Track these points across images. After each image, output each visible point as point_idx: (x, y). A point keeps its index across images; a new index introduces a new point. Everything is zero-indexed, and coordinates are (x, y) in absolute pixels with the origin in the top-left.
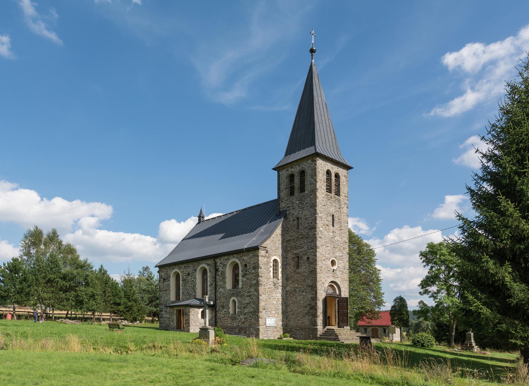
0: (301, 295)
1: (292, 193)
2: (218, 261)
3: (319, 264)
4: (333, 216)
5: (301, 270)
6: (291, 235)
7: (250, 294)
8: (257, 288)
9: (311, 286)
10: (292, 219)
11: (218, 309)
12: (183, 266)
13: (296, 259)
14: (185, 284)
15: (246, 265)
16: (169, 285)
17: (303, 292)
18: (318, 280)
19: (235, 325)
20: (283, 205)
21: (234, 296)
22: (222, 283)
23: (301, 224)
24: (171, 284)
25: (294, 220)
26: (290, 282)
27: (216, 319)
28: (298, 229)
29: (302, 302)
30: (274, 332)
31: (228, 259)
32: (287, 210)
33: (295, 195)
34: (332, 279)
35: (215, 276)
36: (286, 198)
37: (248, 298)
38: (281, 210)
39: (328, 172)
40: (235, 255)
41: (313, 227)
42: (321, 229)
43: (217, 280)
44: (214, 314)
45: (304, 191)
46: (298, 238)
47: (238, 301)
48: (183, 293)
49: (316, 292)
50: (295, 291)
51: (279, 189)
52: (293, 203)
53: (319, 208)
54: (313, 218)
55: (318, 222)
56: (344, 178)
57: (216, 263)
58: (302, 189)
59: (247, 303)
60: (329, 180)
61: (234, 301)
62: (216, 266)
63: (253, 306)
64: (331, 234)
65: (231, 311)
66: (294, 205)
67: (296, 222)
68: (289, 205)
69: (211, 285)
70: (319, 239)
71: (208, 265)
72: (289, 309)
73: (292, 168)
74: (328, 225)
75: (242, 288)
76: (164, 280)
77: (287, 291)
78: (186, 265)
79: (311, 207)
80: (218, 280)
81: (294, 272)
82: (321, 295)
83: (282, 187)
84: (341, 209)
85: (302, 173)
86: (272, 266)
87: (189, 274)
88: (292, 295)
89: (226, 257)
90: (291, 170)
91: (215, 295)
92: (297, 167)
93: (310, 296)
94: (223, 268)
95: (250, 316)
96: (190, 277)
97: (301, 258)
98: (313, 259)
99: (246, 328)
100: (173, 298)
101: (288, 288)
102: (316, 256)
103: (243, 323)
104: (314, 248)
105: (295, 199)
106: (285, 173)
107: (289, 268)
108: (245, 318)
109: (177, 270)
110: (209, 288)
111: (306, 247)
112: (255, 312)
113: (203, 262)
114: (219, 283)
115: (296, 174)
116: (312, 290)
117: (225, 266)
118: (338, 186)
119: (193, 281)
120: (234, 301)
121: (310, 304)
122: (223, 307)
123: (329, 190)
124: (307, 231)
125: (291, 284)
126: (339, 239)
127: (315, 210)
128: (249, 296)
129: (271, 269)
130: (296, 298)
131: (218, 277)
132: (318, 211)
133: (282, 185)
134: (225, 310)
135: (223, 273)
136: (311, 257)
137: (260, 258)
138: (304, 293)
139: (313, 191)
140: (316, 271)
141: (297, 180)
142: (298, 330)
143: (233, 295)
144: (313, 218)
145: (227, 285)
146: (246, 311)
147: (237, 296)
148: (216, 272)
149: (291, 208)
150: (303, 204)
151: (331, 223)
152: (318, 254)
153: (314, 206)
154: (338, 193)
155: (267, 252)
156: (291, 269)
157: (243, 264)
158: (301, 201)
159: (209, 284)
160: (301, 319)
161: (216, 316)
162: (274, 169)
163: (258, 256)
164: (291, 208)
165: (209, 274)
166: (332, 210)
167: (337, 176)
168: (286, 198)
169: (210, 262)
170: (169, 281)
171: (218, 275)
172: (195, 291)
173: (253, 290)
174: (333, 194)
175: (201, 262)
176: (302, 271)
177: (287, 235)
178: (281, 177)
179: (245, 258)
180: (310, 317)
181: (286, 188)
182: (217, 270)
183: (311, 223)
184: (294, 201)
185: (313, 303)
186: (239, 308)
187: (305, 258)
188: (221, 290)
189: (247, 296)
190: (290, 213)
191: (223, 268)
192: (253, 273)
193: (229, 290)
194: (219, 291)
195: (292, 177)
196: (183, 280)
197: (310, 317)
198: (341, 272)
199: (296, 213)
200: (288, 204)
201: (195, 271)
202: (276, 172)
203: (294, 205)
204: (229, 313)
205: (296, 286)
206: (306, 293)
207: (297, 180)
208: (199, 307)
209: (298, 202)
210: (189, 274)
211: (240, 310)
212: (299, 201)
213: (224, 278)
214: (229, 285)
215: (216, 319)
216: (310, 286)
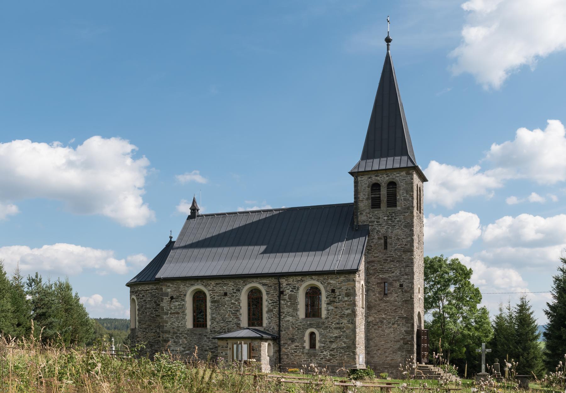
0: (390, 327)
2: (284, 282)
5: (391, 298)
6: (376, 255)
7: (341, 325)
8: (353, 320)
9: (405, 318)
10: (376, 237)
11: (282, 342)
12: (213, 283)
13: (382, 285)
15: (333, 291)
16: (183, 307)
17: (393, 324)
20: (362, 218)
21: (311, 327)
22: (291, 310)
23: (391, 244)
24: (187, 305)
25: (379, 239)
26: (373, 311)
32: (369, 225)
33: (382, 208)
36: (367, 211)
38: (360, 224)
40: (313, 277)
43: (282, 306)
44: (277, 349)
45: (396, 206)
46: (387, 260)
47: (320, 334)
48: (213, 319)
50: (382, 322)
51: (356, 197)
52: (379, 218)
54: (409, 239)
57: (280, 284)
59: (336, 337)
61: (312, 335)
62: (280, 288)
63: (345, 340)
65: (307, 345)
66: (381, 220)
67: (382, 241)
68: (373, 219)
69: (269, 311)
71: (264, 285)
73: (376, 176)
75: (327, 318)
76: (172, 298)
77: (369, 322)
78: (218, 281)
79: (405, 226)
82: (415, 330)
83: (361, 196)
85: (392, 185)
89: (299, 278)
90: (374, 179)
91: (279, 326)
92: (385, 176)
93: (403, 329)
96: (227, 299)
97: (391, 284)
98: (408, 286)
99: (335, 366)
100: (189, 324)
101: (371, 319)
102: (413, 283)
103: (329, 361)
106: (365, 181)
107: (372, 294)
108: (330, 355)
109: (199, 286)
110: (265, 315)
111: (397, 272)
112: (348, 347)
113: (255, 280)
114: (285, 310)
116: (407, 323)
119: (232, 303)
120: (312, 335)
121: (403, 339)
122: (293, 341)
124: (399, 254)
125: (376, 313)
128: (340, 328)
130: (384, 331)
131: (282, 302)
133: (361, 194)
134: (297, 344)
136: (405, 285)
137: (357, 284)
138: (396, 326)
139: (408, 208)
141: (384, 192)
142: (387, 368)
143: (311, 326)
145: (299, 313)
146: (334, 346)
147: (318, 327)
148: (279, 297)
149: (375, 223)
156: (376, 296)
157: (329, 288)
158: (391, 217)
159: (265, 309)
160: (391, 355)
161: (279, 351)
163: (354, 281)
164: (375, 223)
165: (265, 297)
168: (367, 211)
170: (183, 300)
171: (284, 300)
173: (346, 321)
175: (249, 280)
176: (392, 299)
177: (370, 256)
178: (359, 184)
179: (332, 282)
180: (404, 353)
181: (367, 199)
182: (281, 293)
183: (406, 245)
184: (381, 215)
185: (408, 338)
186: (320, 342)
187: (397, 284)
189: (336, 328)
190: (375, 229)
191: (291, 291)
192: (346, 301)
193: (303, 319)
195: (376, 187)
196: (212, 302)
197: (404, 353)
199: (383, 231)
200: (370, 218)
202: (352, 179)
203: (381, 220)
204: (304, 348)
205: (384, 316)
206: (399, 325)
207: (384, 192)
208: (266, 340)
209: (386, 218)
210: (226, 294)
211: (323, 345)
212: (388, 216)
214: (302, 313)
215: (280, 355)
216: (403, 318)
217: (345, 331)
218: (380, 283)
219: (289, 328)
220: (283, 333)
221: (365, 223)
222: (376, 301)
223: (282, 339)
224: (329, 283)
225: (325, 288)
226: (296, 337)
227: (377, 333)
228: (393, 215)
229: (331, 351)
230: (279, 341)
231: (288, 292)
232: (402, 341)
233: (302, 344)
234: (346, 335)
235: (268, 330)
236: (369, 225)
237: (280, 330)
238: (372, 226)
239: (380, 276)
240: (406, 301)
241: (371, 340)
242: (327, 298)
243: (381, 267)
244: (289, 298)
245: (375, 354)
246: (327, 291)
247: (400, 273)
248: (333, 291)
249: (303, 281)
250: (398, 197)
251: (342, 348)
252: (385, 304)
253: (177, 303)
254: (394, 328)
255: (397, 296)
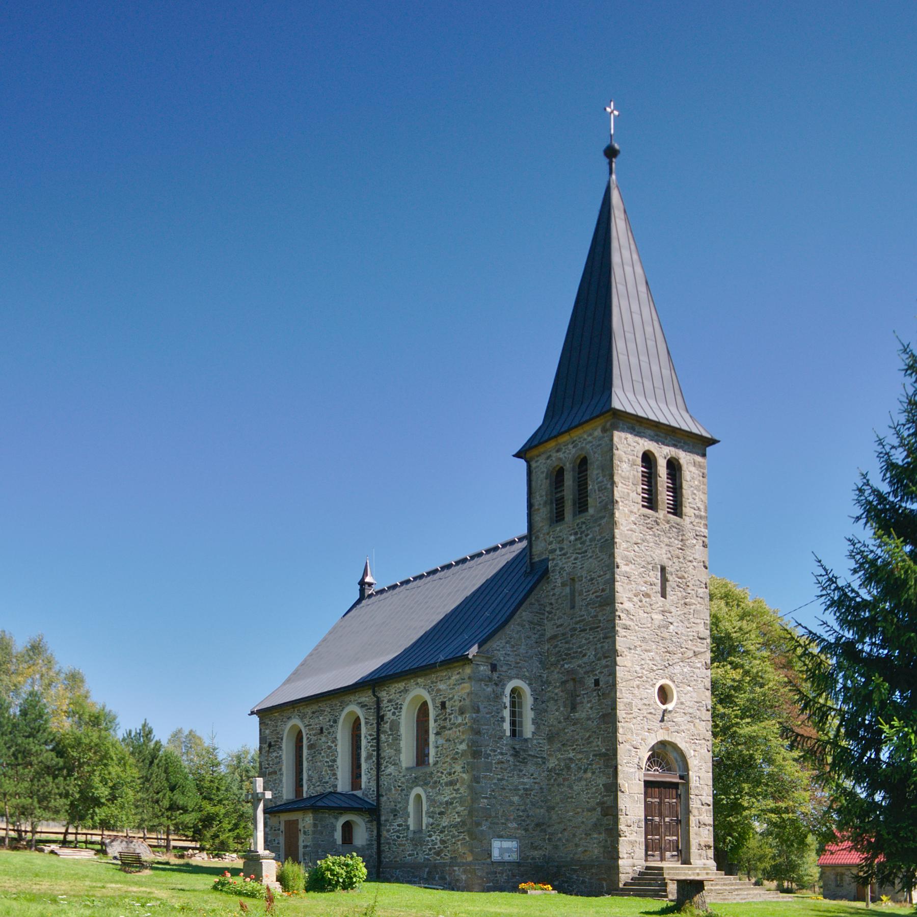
0: (580, 779)
1: (558, 517)
3: (624, 695)
4: (663, 569)
5: (580, 714)
6: (559, 622)
7: (454, 777)
9: (605, 755)
10: (559, 581)
11: (383, 818)
12: (309, 710)
14: (313, 757)
15: (443, 705)
17: (585, 771)
18: (620, 738)
19: (421, 858)
23: (581, 594)
24: (284, 757)
27: (379, 844)
28: (573, 607)
29: (584, 797)
30: (514, 876)
31: (406, 691)
32: (547, 560)
33: (566, 519)
34: (662, 736)
35: (378, 735)
37: (448, 790)
38: (536, 559)
39: (648, 459)
40: (419, 680)
41: (608, 600)
42: (628, 605)
43: (382, 745)
44: (375, 833)
45: (586, 510)
46: (574, 629)
47: (428, 797)
48: (310, 779)
49: (616, 768)
50: (569, 768)
51: (530, 506)
53: (622, 551)
54: (608, 576)
55: (618, 586)
56: (693, 469)
57: (378, 702)
58: (581, 505)
59: (447, 803)
60: (650, 477)
63: (459, 809)
64: (658, 617)
67: (568, 590)
68: (553, 546)
69: (369, 757)
70: (621, 631)
72: (554, 817)
74: (647, 595)
75: (436, 763)
76: (270, 745)
78: (315, 707)
80: (384, 746)
81: (567, 718)
83: (538, 500)
84: (688, 552)
85: (583, 464)
86: (508, 704)
87: (322, 729)
88: (560, 780)
89: (401, 685)
93: (602, 780)
94: (394, 714)
95: (453, 837)
97: (581, 682)
99: (445, 865)
104: (611, 655)
105: (564, 530)
106: (542, 465)
109: (296, 721)
111: (591, 654)
113: (352, 698)
114: (387, 752)
115: (568, 467)
117: (398, 707)
118: (676, 489)
119: (330, 747)
120: (418, 797)
121: (601, 804)
123: (651, 502)
125: (559, 750)
126: (681, 630)
127: (612, 555)
129: (507, 713)
131: (383, 737)
132: (618, 560)
135: (395, 726)
138: (589, 775)
140: (616, 714)
142: (575, 871)
143: (416, 782)
144: (608, 576)
145: (403, 757)
146: (445, 822)
149: (558, 552)
150: (583, 543)
151: (658, 588)
152: (620, 673)
153: (609, 544)
154: (677, 509)
155: (494, 668)
157: (438, 701)
161: (379, 836)
162: (518, 455)
164: (558, 552)
166: (661, 555)
167: (674, 467)
169: (367, 697)
170: (280, 748)
172: (335, 774)
174: (662, 514)
175: (346, 699)
176: (584, 715)
178: (534, 474)
179: (442, 686)
180: (602, 836)
182: (380, 719)
183: (603, 590)
186: (431, 815)
187: (590, 682)
188: (391, 769)
189: (447, 784)
191: (394, 714)
192: (460, 725)
194: (388, 771)
195: (558, 476)
196: (311, 747)
198: (687, 718)
199: (568, 567)
201: (335, 722)
202: (522, 464)
205: (571, 755)
206: (593, 773)
209: (572, 538)
211: (431, 820)
212: (576, 534)
213: (397, 738)
215: (379, 844)
216: (601, 755)
217: (458, 789)
218: (566, 681)
219: (390, 790)
220: (383, 799)
221: (544, 557)
222: (560, 722)
223: (383, 812)
224: (439, 690)
225: (433, 700)
226: (399, 806)
227: (562, 793)
228: (584, 526)
229: (442, 832)
230: (379, 816)
231: (389, 716)
232: (599, 809)
233: (406, 821)
234: (460, 798)
235: (367, 795)
236: (547, 560)
237: (379, 796)
238: (553, 559)
239: (566, 666)
240: (604, 716)
241: (553, 808)
242: (436, 721)
243: (567, 646)
244: (391, 729)
245: (560, 839)
246: (435, 707)
247: (595, 656)
248: (443, 705)
249: (407, 691)
250: (590, 487)
251: (455, 826)
252: (572, 728)
253: (275, 754)
254: (586, 780)
255: (591, 708)
